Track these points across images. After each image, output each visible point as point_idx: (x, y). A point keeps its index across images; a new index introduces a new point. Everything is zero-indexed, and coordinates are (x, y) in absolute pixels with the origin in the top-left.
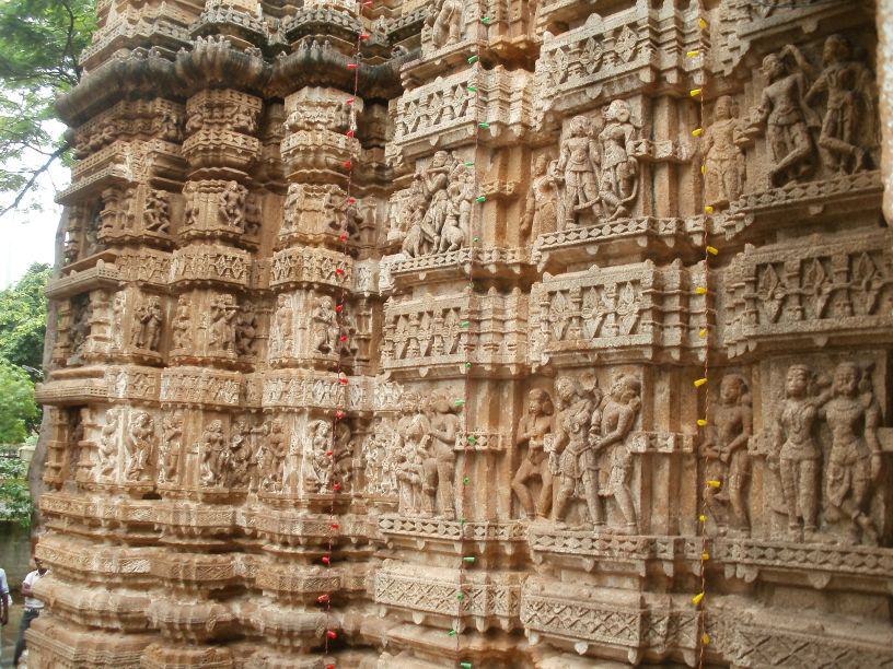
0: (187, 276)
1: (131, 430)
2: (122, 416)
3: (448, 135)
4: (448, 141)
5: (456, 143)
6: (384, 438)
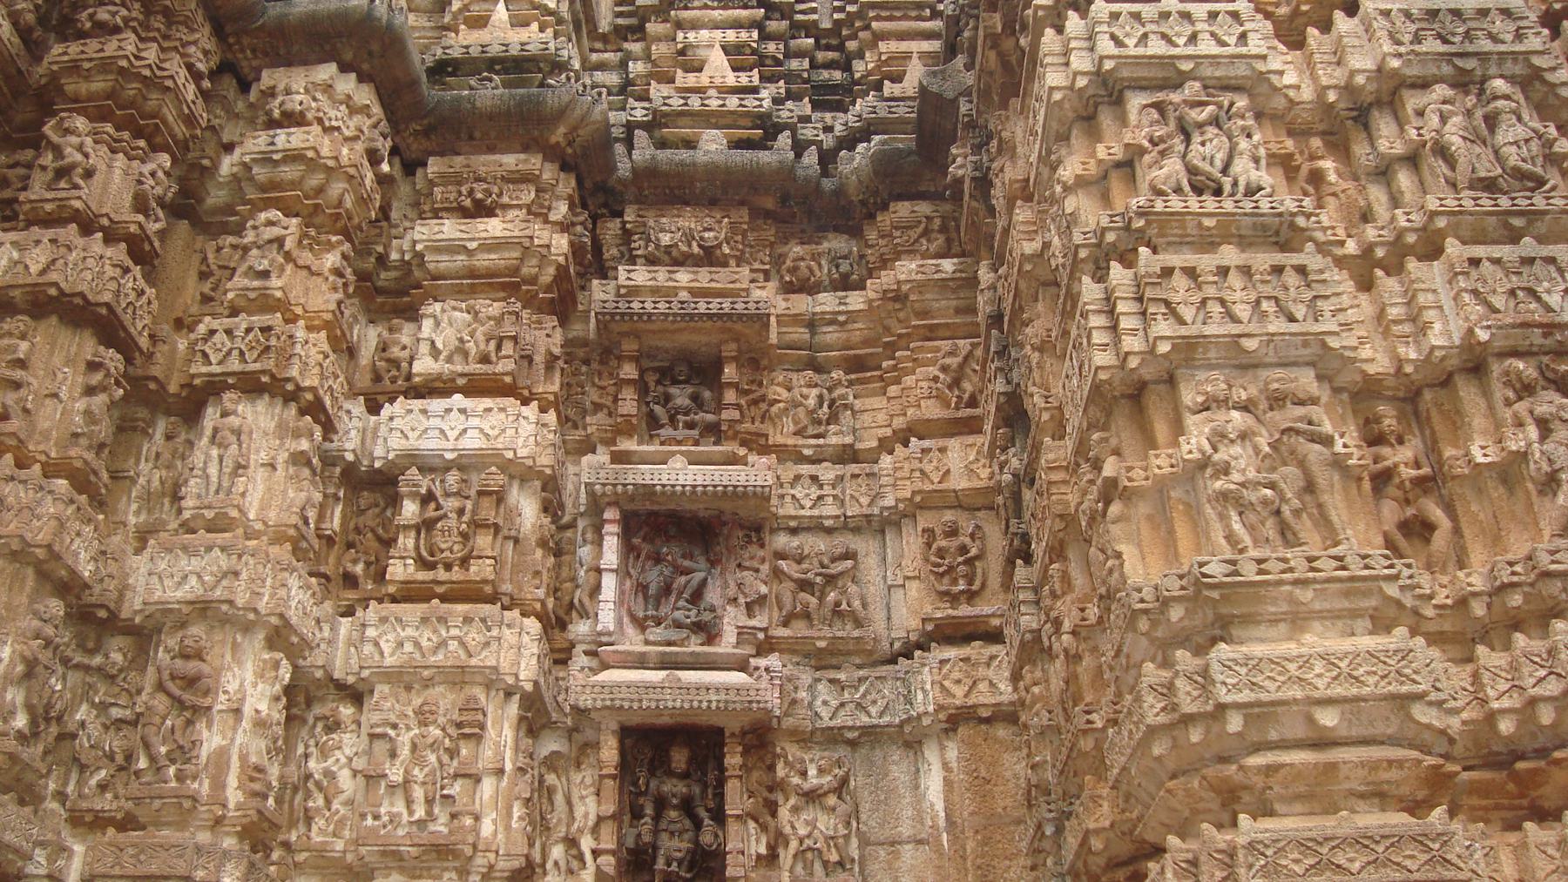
0: (53, 276)
3: (1211, 64)
4: (1208, 71)
5: (1218, 78)
6: (393, 718)
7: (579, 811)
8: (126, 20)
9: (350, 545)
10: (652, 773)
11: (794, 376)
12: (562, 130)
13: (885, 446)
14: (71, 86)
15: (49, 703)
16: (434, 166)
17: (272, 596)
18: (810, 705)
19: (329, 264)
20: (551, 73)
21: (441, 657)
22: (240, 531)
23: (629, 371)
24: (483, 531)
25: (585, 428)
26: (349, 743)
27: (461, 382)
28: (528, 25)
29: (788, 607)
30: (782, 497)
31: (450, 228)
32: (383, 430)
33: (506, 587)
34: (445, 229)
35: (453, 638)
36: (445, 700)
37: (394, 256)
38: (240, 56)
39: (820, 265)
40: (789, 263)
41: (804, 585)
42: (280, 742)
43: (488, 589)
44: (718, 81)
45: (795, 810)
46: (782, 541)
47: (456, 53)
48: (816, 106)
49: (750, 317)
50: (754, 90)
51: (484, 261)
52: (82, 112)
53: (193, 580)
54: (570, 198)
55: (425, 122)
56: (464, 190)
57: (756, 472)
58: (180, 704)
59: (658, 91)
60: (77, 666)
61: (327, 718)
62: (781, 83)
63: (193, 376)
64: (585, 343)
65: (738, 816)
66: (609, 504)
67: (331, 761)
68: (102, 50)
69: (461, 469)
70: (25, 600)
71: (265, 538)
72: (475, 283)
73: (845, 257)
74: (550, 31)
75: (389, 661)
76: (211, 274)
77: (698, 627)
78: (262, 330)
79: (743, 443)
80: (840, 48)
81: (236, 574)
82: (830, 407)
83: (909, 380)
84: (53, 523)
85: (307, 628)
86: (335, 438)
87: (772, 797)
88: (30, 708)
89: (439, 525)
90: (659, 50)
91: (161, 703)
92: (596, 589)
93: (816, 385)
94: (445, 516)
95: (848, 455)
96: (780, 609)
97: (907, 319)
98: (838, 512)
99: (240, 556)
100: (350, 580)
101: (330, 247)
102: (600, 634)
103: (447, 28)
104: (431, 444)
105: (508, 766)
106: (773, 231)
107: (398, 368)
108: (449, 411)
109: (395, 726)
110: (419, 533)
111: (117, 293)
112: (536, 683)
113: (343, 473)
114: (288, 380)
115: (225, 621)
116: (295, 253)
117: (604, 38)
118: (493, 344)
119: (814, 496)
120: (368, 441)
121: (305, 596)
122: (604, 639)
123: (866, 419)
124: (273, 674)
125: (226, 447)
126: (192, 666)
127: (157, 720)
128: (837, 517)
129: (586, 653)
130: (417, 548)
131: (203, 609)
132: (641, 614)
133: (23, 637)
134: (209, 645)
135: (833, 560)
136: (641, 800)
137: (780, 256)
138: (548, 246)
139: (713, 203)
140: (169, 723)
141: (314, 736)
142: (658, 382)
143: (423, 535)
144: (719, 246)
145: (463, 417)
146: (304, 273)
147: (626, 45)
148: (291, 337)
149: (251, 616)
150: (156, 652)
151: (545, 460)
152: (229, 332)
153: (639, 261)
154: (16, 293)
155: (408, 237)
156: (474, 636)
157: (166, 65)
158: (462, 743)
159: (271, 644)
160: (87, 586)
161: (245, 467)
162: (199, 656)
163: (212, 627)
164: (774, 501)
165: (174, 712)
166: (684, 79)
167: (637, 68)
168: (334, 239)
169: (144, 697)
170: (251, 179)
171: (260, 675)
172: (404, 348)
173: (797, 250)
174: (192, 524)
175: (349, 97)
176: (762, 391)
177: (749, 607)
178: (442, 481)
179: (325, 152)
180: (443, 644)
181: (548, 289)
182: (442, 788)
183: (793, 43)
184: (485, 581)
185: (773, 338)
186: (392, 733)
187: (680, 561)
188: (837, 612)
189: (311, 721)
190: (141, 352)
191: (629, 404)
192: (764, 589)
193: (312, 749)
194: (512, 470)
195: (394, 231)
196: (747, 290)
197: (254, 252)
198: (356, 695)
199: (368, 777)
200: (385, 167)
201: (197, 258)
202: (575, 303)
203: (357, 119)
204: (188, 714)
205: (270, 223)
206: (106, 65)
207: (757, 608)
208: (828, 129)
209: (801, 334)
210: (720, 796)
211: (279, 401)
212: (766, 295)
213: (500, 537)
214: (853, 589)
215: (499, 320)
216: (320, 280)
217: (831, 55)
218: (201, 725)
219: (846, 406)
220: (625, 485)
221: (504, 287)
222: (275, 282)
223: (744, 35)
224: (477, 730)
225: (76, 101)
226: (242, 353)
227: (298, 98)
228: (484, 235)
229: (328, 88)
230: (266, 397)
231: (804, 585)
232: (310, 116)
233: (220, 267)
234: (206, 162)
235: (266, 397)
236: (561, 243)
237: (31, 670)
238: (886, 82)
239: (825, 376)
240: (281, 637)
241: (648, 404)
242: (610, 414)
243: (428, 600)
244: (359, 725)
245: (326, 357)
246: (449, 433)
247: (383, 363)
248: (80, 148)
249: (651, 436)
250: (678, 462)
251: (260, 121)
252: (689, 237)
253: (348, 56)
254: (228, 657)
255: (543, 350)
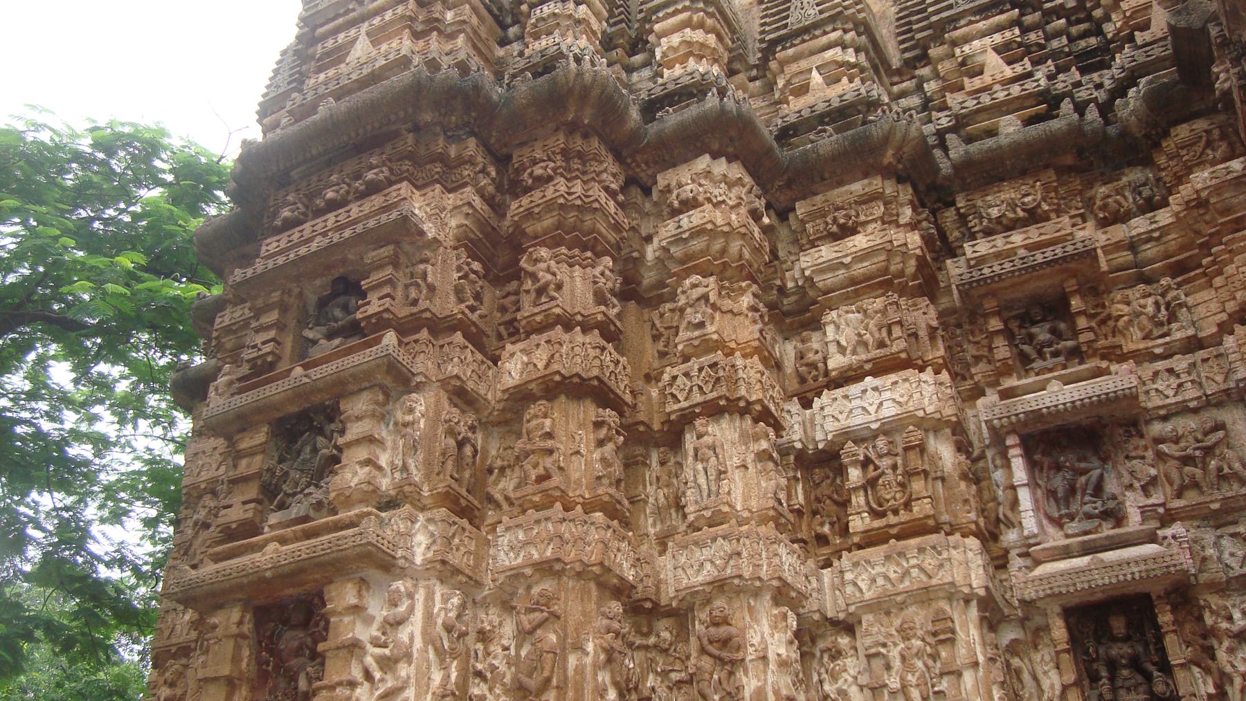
0: (555, 367)
1: (440, 621)
2: (420, 596)
6: (882, 639)
7: (1046, 684)
8: (554, 170)
9: (815, 513)
10: (1098, 642)
11: (1129, 292)
12: (890, 152)
13: (1225, 328)
14: (531, 228)
15: (628, 678)
16: (801, 209)
17: (769, 565)
18: (1219, 559)
19: (745, 305)
20: (868, 111)
21: (907, 583)
22: (733, 521)
23: (995, 324)
24: (915, 478)
25: (972, 378)
26: (852, 665)
27: (868, 367)
28: (839, 80)
29: (1177, 482)
30: (1147, 392)
31: (826, 252)
32: (818, 419)
33: (945, 518)
34: (823, 253)
35: (913, 567)
36: (919, 616)
37: (790, 285)
38: (638, 170)
39: (1125, 197)
40: (1098, 203)
41: (1186, 460)
42: (801, 675)
43: (931, 522)
44: (998, 77)
45: (1231, 651)
46: (1157, 428)
47: (792, 119)
48: (1083, 71)
49: (1080, 255)
50: (1029, 75)
51: (860, 269)
52: (543, 244)
53: (708, 566)
54: (911, 202)
55: (785, 177)
56: (829, 220)
57: (1120, 378)
58: (721, 661)
59: (953, 100)
60: (639, 647)
61: (830, 650)
62: (1050, 62)
63: (669, 414)
64: (954, 311)
65: (1182, 665)
66: (1008, 433)
67: (840, 682)
68: (544, 196)
69: (886, 433)
70: (594, 606)
71: (753, 522)
72: (857, 288)
73: (1144, 185)
74: (857, 81)
75: (868, 595)
76: (661, 335)
77: (1106, 515)
78: (710, 366)
79: (1103, 357)
80: (1089, 18)
81: (739, 554)
82: (1167, 309)
83: (1230, 269)
84: (600, 546)
85: (800, 584)
86: (784, 433)
87: (1207, 643)
88: (616, 684)
89: (880, 481)
90: (944, 67)
91: (706, 663)
92: (1015, 503)
93: (1150, 295)
94: (883, 473)
95: (1193, 344)
96: (1171, 484)
97: (1214, 219)
98: (1199, 394)
99: (738, 540)
100: (822, 540)
101: (743, 291)
102: (1028, 538)
103: (779, 102)
104: (858, 420)
105: (981, 659)
106: (1078, 182)
107: (816, 368)
108: (864, 391)
109: (884, 645)
110: (866, 491)
111: (601, 367)
112: (987, 588)
113: (796, 459)
114: (739, 399)
115: (739, 591)
116: (719, 303)
117: (899, 72)
118: (884, 333)
119: (1174, 386)
120: (809, 430)
121: (793, 560)
122: (1032, 541)
123: (1201, 311)
124: (784, 624)
125: (707, 461)
126: (723, 631)
127: (707, 676)
128: (1199, 398)
129: (1020, 555)
130: (868, 503)
131: (720, 585)
132: (1056, 515)
133: (599, 634)
134: (731, 612)
135: (1206, 434)
136: (1095, 666)
137: (1090, 199)
138: (906, 244)
139: (1023, 173)
140: (716, 677)
141: (822, 665)
142: (1020, 327)
143: (869, 492)
144: (1039, 205)
145: (877, 394)
146: (729, 316)
147: (918, 72)
148: (733, 366)
149: (758, 584)
150: (694, 626)
151: (949, 411)
152: (686, 375)
153: (979, 235)
154: (533, 386)
155: (797, 267)
156: (929, 562)
157: (590, 193)
158: (940, 648)
159: (777, 602)
160: (634, 587)
161: (725, 472)
162: (726, 622)
163: (731, 598)
164: (1142, 398)
165: (718, 668)
166: (971, 84)
167: (931, 87)
168: (744, 284)
169: (693, 660)
170: (671, 257)
171: (774, 627)
172: (817, 352)
173: (1103, 190)
174: (696, 524)
175: (724, 175)
176: (1107, 311)
177: (1145, 490)
178: (874, 447)
179: (719, 222)
180: (907, 573)
181: (914, 277)
182: (933, 686)
183: (1048, 27)
184: (928, 517)
185: (1104, 266)
186: (883, 650)
187: (1077, 465)
188: (1222, 477)
189: (818, 654)
190: (626, 404)
191: (1002, 350)
192: (1153, 472)
193: (824, 676)
194: (925, 425)
195: (784, 266)
196: (1071, 234)
197: (689, 310)
198: (848, 627)
199: (873, 689)
200: (766, 220)
201: (648, 326)
202: (937, 282)
203: (736, 191)
204: (728, 667)
205: (694, 286)
206: (550, 206)
207: (1151, 488)
208: (1099, 86)
209: (1125, 257)
210: (1162, 651)
211: (737, 417)
212: (1088, 233)
213: (930, 479)
214: (1229, 454)
215: (884, 312)
216: (742, 318)
217: (1083, 27)
218: (740, 674)
219: (1180, 305)
220: (1016, 415)
221: (880, 284)
222: (710, 328)
223: (1008, 34)
224: (950, 635)
225: (536, 238)
226: (700, 388)
227: (688, 188)
228: (854, 250)
229: (708, 174)
230: (727, 415)
231: (1186, 460)
232: (700, 198)
233: (666, 328)
234: (635, 254)
235: (727, 415)
236: (914, 239)
237: (610, 658)
238: (1136, 33)
239: (1155, 286)
240: (783, 595)
241: (1016, 346)
242: (989, 362)
243: (886, 541)
244: (856, 650)
245: (763, 374)
246: (869, 409)
247: (804, 368)
248: (548, 270)
249: (1027, 371)
250: (1055, 386)
251: (665, 213)
252: (1013, 206)
253: (716, 146)
254: (748, 618)
255: (923, 325)
